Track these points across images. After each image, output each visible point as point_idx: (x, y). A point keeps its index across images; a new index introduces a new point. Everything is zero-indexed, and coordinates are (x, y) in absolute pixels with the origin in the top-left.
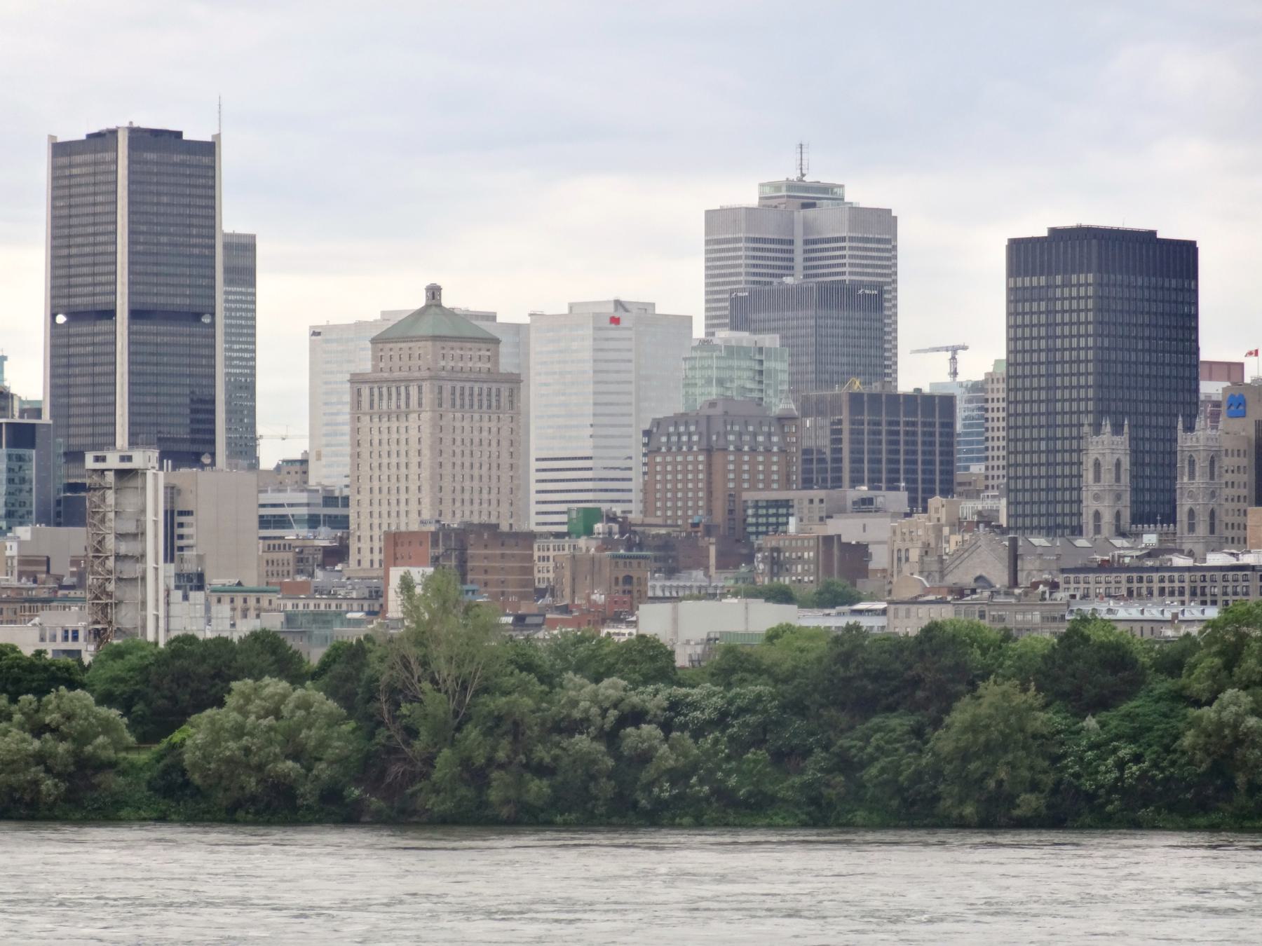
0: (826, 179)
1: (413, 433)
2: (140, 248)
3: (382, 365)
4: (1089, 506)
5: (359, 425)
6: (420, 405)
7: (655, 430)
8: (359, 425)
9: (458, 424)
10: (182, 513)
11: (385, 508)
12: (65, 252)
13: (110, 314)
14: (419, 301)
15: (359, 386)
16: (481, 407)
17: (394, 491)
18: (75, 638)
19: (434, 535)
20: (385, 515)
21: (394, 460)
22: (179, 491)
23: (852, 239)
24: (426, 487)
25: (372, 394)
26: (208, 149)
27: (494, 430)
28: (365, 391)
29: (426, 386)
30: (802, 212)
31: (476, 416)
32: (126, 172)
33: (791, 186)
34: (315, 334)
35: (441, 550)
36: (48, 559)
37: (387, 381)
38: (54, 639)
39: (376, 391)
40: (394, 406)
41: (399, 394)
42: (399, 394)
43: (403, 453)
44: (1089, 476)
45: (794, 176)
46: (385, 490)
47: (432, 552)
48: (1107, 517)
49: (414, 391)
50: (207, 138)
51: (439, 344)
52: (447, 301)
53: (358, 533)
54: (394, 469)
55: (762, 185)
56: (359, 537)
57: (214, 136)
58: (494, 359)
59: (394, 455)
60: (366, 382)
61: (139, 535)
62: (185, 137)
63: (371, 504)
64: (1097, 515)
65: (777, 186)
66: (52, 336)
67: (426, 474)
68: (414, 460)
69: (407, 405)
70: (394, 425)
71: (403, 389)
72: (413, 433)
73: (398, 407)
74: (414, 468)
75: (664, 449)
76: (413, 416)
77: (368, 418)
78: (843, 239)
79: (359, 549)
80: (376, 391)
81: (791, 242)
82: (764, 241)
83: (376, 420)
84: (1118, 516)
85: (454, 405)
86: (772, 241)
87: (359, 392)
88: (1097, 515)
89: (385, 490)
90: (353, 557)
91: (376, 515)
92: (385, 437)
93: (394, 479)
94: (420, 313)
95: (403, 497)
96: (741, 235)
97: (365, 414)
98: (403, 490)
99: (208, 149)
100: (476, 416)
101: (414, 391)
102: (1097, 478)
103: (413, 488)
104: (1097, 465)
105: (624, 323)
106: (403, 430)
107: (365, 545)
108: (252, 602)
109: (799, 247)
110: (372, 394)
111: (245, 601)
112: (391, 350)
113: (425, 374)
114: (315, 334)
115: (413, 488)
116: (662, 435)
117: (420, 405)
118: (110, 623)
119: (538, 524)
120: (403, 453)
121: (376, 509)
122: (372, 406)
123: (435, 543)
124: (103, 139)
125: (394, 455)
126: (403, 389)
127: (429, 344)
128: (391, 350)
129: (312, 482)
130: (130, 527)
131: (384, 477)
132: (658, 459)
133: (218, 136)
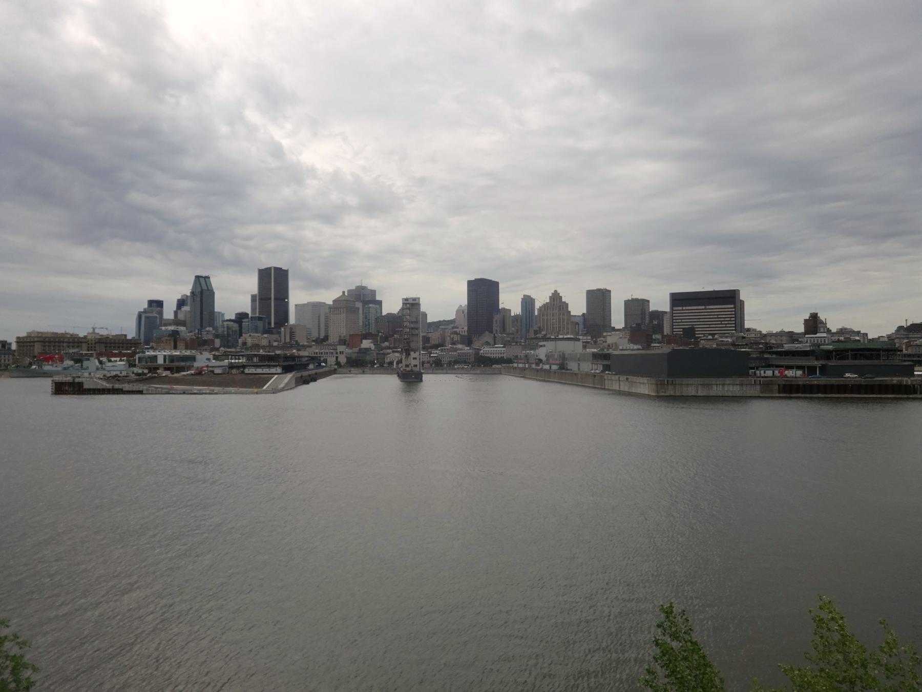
0: (365, 285)
4: (495, 328)
13: (270, 299)
14: (341, 294)
26: (286, 272)
28: (332, 310)
29: (345, 309)
33: (360, 286)
34: (296, 305)
38: (312, 354)
44: (494, 323)
45: (360, 285)
48: (499, 331)
49: (342, 310)
61: (417, 322)
64: (496, 330)
65: (358, 286)
67: (344, 324)
84: (500, 331)
87: (330, 310)
88: (496, 330)
90: (329, 341)
94: (341, 296)
99: (286, 272)
101: (342, 310)
102: (496, 323)
104: (496, 321)
107: (332, 338)
109: (362, 296)
114: (296, 305)
118: (410, 347)
124: (269, 269)
130: (414, 320)
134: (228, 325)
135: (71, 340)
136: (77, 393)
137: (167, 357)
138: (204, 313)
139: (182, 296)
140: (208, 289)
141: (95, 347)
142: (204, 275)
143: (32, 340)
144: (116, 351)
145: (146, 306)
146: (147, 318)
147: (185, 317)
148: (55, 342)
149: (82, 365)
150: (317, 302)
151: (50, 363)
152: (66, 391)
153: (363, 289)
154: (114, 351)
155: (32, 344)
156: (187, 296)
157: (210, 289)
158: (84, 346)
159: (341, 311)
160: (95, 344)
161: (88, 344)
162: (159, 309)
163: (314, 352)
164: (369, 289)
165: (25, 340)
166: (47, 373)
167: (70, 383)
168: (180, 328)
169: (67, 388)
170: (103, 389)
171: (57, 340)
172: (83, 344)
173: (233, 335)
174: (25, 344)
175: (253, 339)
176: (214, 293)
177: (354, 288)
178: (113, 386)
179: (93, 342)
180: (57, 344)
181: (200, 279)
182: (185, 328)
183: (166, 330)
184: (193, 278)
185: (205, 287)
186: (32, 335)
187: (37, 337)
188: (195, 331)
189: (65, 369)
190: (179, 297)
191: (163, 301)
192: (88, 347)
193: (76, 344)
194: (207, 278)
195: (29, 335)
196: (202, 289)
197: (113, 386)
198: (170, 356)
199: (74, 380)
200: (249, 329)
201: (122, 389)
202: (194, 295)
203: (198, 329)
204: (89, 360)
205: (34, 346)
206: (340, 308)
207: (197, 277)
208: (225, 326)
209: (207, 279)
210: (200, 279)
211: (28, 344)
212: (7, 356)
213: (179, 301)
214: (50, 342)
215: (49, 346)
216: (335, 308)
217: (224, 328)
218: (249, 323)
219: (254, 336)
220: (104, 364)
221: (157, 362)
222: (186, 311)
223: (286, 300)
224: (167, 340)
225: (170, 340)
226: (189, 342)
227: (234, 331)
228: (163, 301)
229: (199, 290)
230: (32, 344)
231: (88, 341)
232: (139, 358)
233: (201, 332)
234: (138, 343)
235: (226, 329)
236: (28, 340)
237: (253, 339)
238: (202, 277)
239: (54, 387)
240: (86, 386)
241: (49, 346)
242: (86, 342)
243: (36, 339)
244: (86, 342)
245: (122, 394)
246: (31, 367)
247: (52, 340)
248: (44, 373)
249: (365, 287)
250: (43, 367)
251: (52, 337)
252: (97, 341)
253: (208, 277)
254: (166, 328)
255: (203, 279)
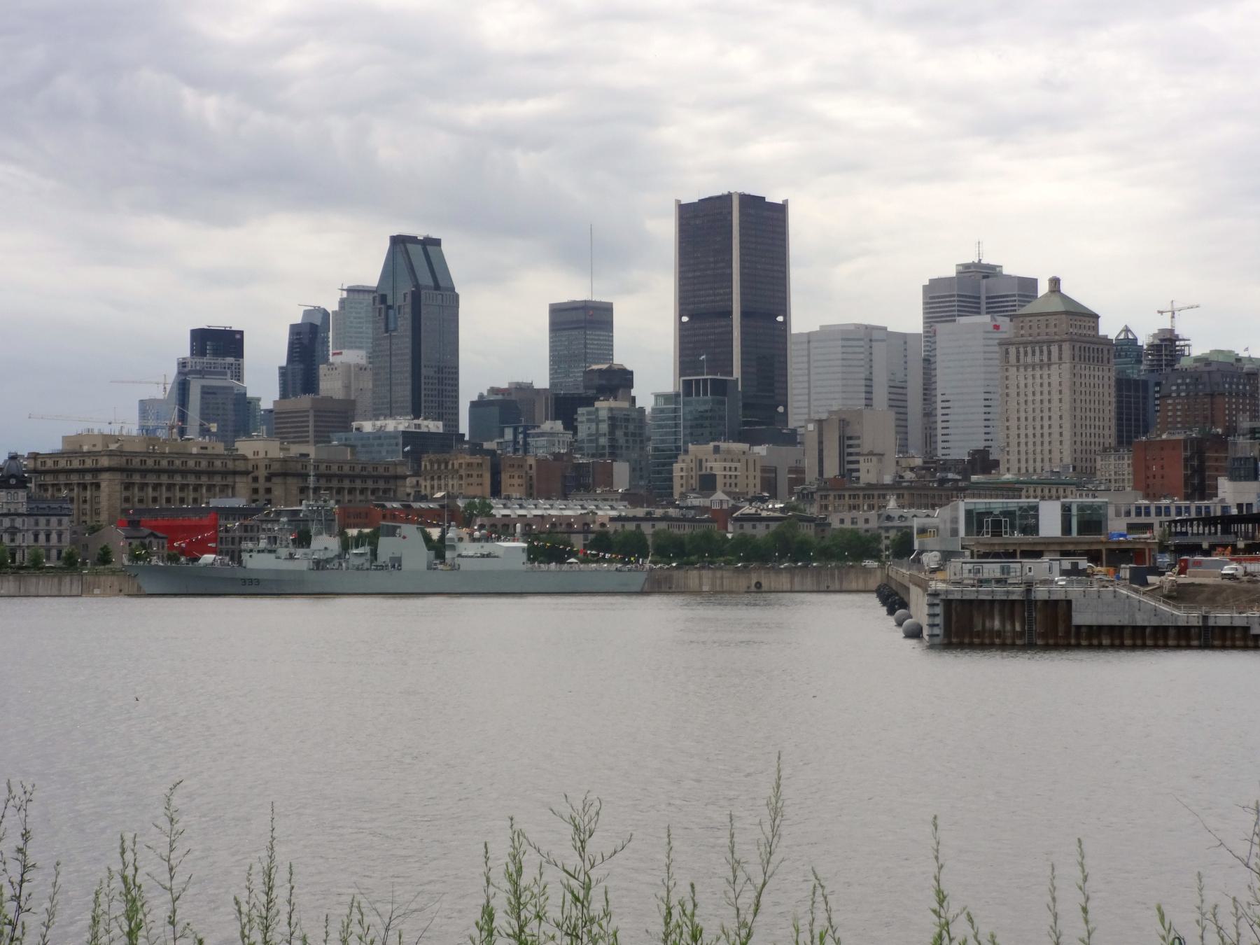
0: (993, 262)
1: (1055, 379)
2: (746, 271)
3: (1023, 332)
5: (1008, 374)
6: (1060, 358)
7: (1164, 382)
8: (1008, 374)
9: (1083, 373)
10: (850, 438)
11: (1030, 432)
12: (690, 275)
13: (728, 314)
15: (1006, 347)
16: (1098, 361)
17: (1038, 419)
18: (1148, 514)
19: (1185, 441)
20: (1031, 436)
21: (1038, 397)
22: (848, 423)
23: (1019, 295)
24: (1067, 416)
25: (1018, 352)
26: (780, 210)
27: (1101, 377)
28: (1012, 350)
29: (1066, 346)
30: (985, 281)
31: (1092, 367)
32: (738, 221)
33: (973, 264)
35: (1189, 453)
36: (776, 468)
37: (1031, 342)
39: (1022, 350)
40: (1037, 359)
41: (1041, 352)
42: (1041, 352)
43: (1046, 392)
45: (976, 261)
46: (1030, 419)
47: (1183, 454)
49: (1055, 349)
50: (781, 203)
51: (1071, 317)
52: (1065, 289)
53: (1007, 449)
54: (1038, 405)
55: (958, 265)
56: (1008, 452)
57: (783, 201)
58: (1096, 328)
59: (1038, 394)
60: (1013, 344)
62: (767, 200)
63: (1019, 429)
65: (967, 266)
66: (680, 330)
67: (1066, 406)
68: (1056, 397)
69: (1049, 359)
70: (1038, 373)
71: (1045, 348)
72: (1055, 379)
73: (1042, 360)
74: (1055, 403)
75: (1174, 395)
76: (1054, 367)
77: (1015, 369)
78: (1014, 296)
79: (1008, 460)
80: (1022, 350)
81: (979, 298)
82: (966, 296)
83: (1022, 369)
85: (1080, 360)
86: (970, 297)
87: (1007, 352)
89: (1030, 419)
91: (1023, 436)
92: (1030, 381)
93: (1038, 411)
95: (1046, 423)
96: (955, 293)
97: (1012, 366)
98: (1046, 418)
99: (780, 210)
100: (1092, 367)
101: (1055, 349)
103: (1055, 417)
105: (1002, 329)
106: (1045, 377)
108: (1046, 491)
110: (1018, 352)
111: (1042, 491)
112: (1030, 321)
113: (1065, 337)
115: (1055, 417)
116: (1172, 385)
117: (1060, 358)
119: (943, 455)
120: (1046, 392)
121: (1023, 432)
122: (1018, 360)
123: (1186, 449)
124: (726, 199)
125: (1038, 394)
126: (1045, 348)
127: (1064, 316)
128: (1030, 321)
129: (789, 427)
131: (1030, 410)
132: (1170, 401)
133: (786, 201)
134: (611, 409)
135: (204, 464)
136: (1040, 642)
137: (1074, 511)
138: (424, 371)
139: (307, 313)
140: (437, 287)
141: (268, 491)
142: (420, 233)
143: (89, 463)
144: (395, 505)
145: (185, 350)
146: (206, 392)
147: (347, 387)
148: (159, 472)
149: (374, 554)
150: (858, 326)
151: (263, 544)
152: (999, 634)
153: (986, 277)
154: (388, 505)
155: (88, 478)
156: (325, 314)
157: (442, 284)
158: (243, 484)
159: (1049, 353)
160: (268, 479)
161: (256, 479)
162: (230, 360)
163: (1138, 509)
164: (1009, 277)
165: (62, 464)
166: (258, 582)
167: (1013, 602)
168: (426, 423)
169: (997, 624)
170: (1156, 628)
171: (164, 463)
172: (238, 479)
173: (628, 448)
174: (62, 479)
175: (728, 465)
176: (457, 296)
177: (952, 273)
178: (1205, 618)
179: (262, 473)
180: (164, 479)
181: (410, 247)
182: (440, 424)
183: (380, 435)
184: (387, 244)
185: (425, 279)
186: (85, 448)
187: (111, 454)
188: (502, 436)
189: (319, 565)
190: (298, 320)
191: (241, 333)
192: (255, 491)
193: (217, 480)
194: (430, 244)
195: (73, 450)
196: (417, 286)
197: (1205, 618)
198: (1081, 508)
199: (1028, 591)
200: (676, 426)
201: (1246, 629)
202: (389, 307)
203: (516, 429)
204: (392, 532)
205: (98, 486)
206: (1050, 343)
207: (399, 242)
208: (604, 414)
209: (430, 248)
210: (410, 247)
211: (75, 479)
212: (54, 520)
213: (296, 331)
214: (144, 472)
215: (143, 487)
216: (1025, 344)
217: (598, 421)
218: (676, 403)
219: (729, 451)
220: (453, 548)
221: (1037, 534)
222: (348, 367)
223: (780, 319)
224: (469, 465)
225: (479, 465)
226: (533, 472)
227: (634, 435)
228: (241, 333)
229: (406, 288)
230: (88, 478)
231: (256, 467)
232: (969, 513)
233: (526, 436)
234: (396, 477)
235: (604, 427)
236: (76, 464)
237: (728, 465)
238: (413, 240)
239: (938, 620)
240: (1079, 619)
241: (170, 487)
242: (246, 473)
243: (105, 462)
244: (246, 473)
245: (1245, 648)
246: (197, 559)
247: (136, 462)
248: (245, 581)
249: (993, 267)
250: (245, 556)
251: (148, 454)
252: (276, 467)
253: (437, 242)
254: (378, 423)
255: (419, 247)
